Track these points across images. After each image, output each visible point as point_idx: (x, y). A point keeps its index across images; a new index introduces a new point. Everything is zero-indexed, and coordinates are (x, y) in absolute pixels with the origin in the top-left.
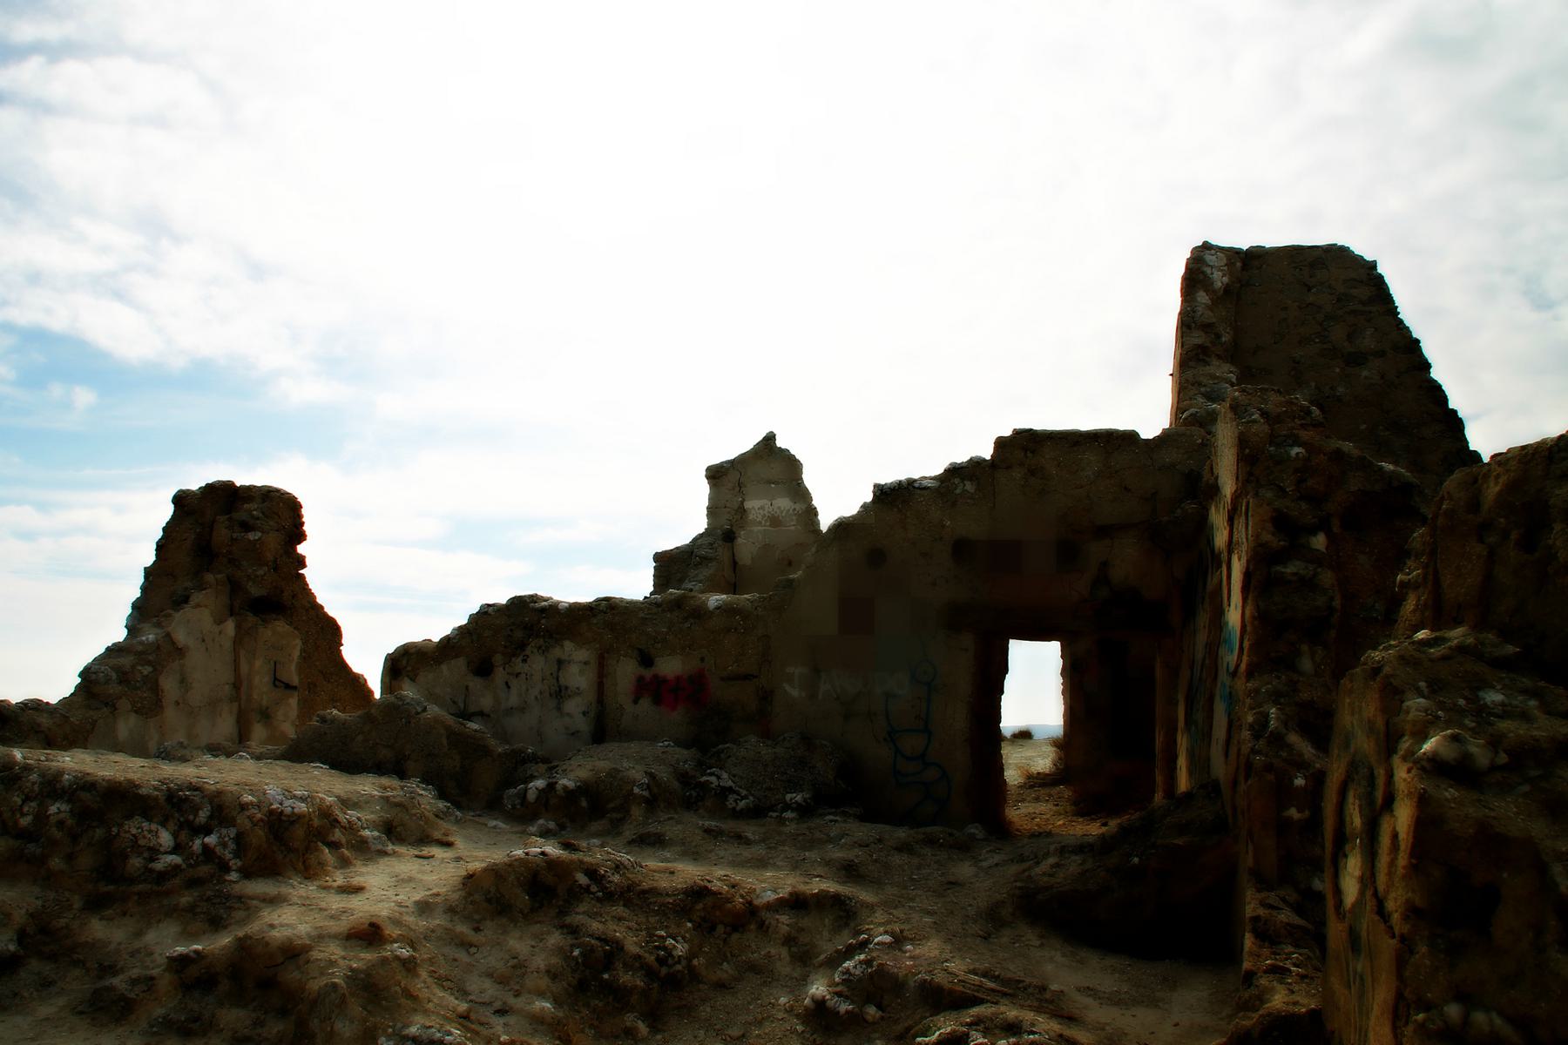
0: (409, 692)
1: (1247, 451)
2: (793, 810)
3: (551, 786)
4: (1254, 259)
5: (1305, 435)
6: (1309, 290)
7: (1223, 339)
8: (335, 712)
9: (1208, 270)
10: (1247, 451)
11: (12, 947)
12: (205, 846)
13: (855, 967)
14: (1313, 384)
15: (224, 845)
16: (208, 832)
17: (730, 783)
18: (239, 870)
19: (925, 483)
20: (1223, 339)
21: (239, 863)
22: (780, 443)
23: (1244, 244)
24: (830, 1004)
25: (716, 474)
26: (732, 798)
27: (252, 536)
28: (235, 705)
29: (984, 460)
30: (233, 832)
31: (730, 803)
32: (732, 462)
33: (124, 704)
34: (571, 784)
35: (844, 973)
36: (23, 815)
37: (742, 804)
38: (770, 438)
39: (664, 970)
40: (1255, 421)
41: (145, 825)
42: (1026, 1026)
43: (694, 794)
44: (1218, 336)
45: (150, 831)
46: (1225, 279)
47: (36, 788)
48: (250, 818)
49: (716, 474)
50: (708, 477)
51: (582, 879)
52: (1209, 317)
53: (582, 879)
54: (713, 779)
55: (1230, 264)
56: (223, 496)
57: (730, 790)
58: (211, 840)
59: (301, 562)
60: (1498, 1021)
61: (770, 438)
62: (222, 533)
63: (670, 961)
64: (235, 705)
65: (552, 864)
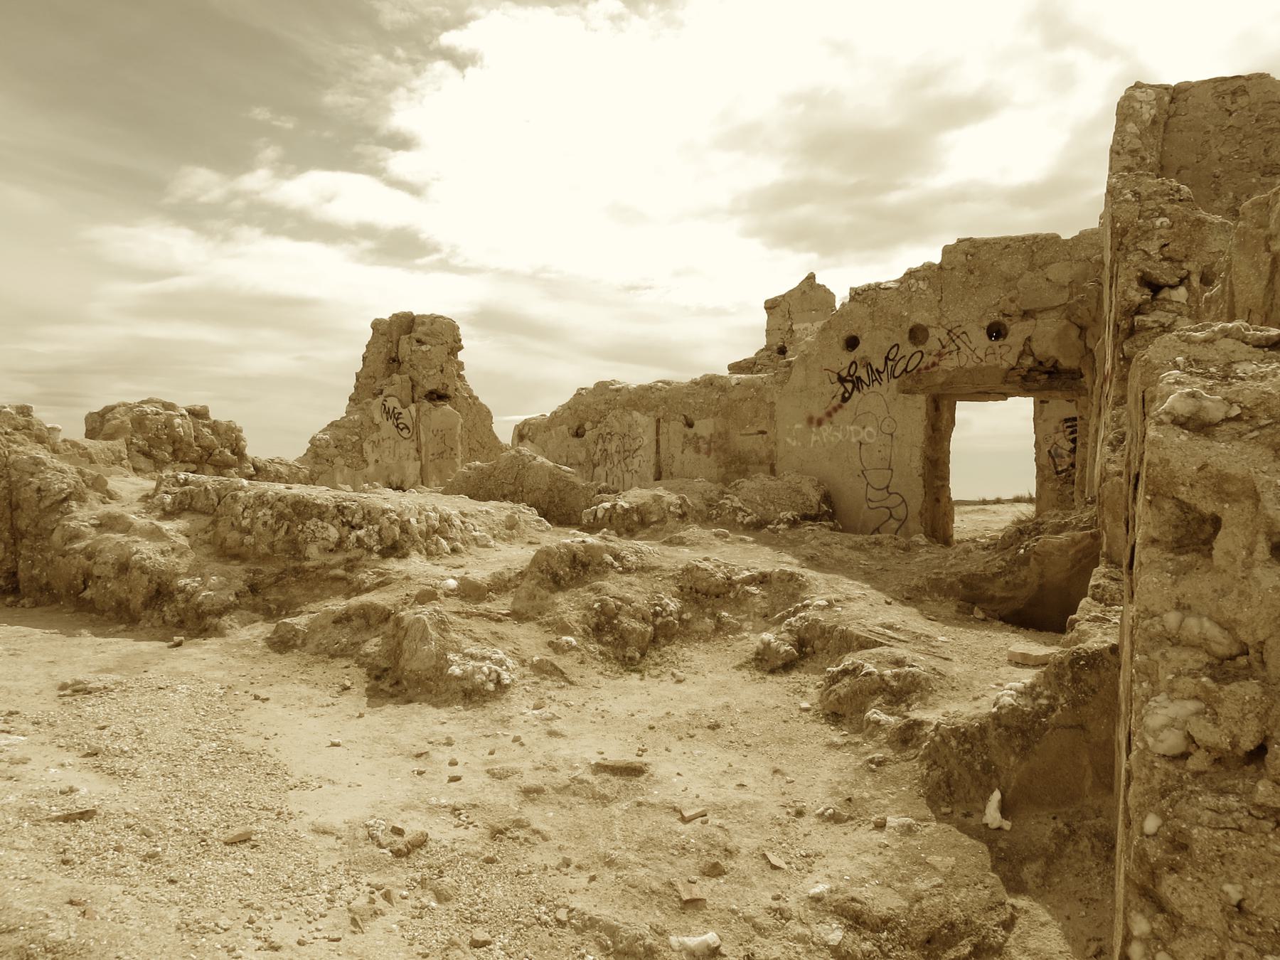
0: (526, 449)
1: (1118, 225)
2: (784, 523)
3: (614, 507)
4: (1177, 94)
5: (1169, 208)
6: (1230, 115)
7: (1148, 161)
8: (478, 463)
9: (1137, 106)
10: (1118, 225)
11: (231, 599)
12: (358, 539)
13: (796, 621)
14: (1231, 194)
15: (370, 536)
16: (361, 528)
17: (740, 504)
18: (379, 552)
19: (889, 285)
20: (1148, 161)
21: (380, 547)
22: (819, 281)
23: (1173, 81)
24: (774, 645)
25: (771, 306)
26: (740, 514)
27: (424, 348)
28: (419, 463)
29: (934, 265)
30: (376, 528)
31: (739, 519)
32: (783, 296)
33: (339, 461)
34: (626, 506)
35: (787, 625)
36: (244, 518)
37: (748, 519)
38: (811, 277)
39: (659, 620)
40: (1126, 201)
41: (320, 523)
42: (908, 661)
43: (715, 512)
44: (1143, 159)
45: (323, 528)
46: (1153, 112)
47: (251, 501)
48: (389, 519)
49: (771, 306)
50: (766, 308)
51: (609, 558)
52: (1137, 144)
53: (609, 558)
54: (728, 502)
55: (1159, 99)
56: (406, 324)
57: (740, 509)
58: (361, 533)
59: (461, 366)
60: (1207, 624)
61: (811, 277)
62: (405, 348)
63: (664, 614)
64: (419, 463)
65: (588, 548)
